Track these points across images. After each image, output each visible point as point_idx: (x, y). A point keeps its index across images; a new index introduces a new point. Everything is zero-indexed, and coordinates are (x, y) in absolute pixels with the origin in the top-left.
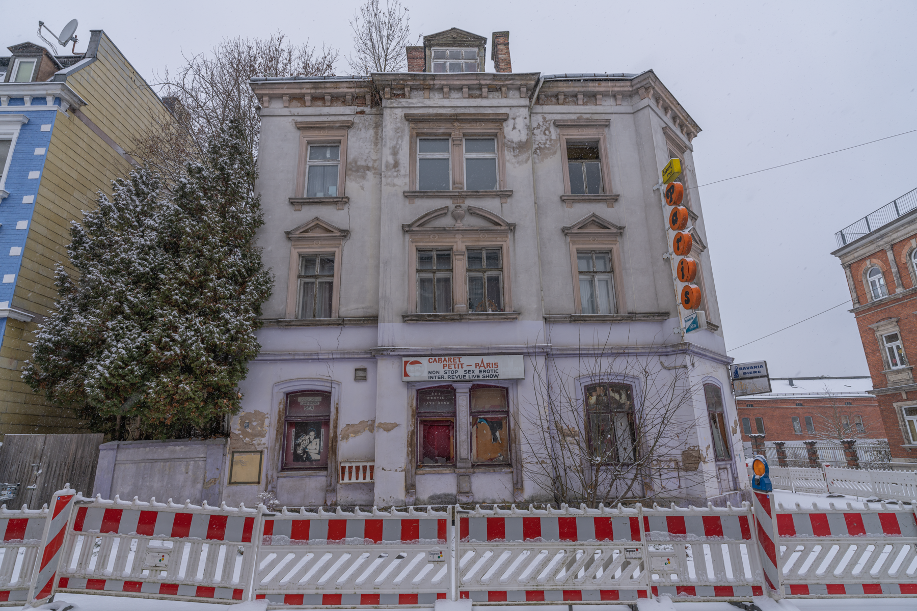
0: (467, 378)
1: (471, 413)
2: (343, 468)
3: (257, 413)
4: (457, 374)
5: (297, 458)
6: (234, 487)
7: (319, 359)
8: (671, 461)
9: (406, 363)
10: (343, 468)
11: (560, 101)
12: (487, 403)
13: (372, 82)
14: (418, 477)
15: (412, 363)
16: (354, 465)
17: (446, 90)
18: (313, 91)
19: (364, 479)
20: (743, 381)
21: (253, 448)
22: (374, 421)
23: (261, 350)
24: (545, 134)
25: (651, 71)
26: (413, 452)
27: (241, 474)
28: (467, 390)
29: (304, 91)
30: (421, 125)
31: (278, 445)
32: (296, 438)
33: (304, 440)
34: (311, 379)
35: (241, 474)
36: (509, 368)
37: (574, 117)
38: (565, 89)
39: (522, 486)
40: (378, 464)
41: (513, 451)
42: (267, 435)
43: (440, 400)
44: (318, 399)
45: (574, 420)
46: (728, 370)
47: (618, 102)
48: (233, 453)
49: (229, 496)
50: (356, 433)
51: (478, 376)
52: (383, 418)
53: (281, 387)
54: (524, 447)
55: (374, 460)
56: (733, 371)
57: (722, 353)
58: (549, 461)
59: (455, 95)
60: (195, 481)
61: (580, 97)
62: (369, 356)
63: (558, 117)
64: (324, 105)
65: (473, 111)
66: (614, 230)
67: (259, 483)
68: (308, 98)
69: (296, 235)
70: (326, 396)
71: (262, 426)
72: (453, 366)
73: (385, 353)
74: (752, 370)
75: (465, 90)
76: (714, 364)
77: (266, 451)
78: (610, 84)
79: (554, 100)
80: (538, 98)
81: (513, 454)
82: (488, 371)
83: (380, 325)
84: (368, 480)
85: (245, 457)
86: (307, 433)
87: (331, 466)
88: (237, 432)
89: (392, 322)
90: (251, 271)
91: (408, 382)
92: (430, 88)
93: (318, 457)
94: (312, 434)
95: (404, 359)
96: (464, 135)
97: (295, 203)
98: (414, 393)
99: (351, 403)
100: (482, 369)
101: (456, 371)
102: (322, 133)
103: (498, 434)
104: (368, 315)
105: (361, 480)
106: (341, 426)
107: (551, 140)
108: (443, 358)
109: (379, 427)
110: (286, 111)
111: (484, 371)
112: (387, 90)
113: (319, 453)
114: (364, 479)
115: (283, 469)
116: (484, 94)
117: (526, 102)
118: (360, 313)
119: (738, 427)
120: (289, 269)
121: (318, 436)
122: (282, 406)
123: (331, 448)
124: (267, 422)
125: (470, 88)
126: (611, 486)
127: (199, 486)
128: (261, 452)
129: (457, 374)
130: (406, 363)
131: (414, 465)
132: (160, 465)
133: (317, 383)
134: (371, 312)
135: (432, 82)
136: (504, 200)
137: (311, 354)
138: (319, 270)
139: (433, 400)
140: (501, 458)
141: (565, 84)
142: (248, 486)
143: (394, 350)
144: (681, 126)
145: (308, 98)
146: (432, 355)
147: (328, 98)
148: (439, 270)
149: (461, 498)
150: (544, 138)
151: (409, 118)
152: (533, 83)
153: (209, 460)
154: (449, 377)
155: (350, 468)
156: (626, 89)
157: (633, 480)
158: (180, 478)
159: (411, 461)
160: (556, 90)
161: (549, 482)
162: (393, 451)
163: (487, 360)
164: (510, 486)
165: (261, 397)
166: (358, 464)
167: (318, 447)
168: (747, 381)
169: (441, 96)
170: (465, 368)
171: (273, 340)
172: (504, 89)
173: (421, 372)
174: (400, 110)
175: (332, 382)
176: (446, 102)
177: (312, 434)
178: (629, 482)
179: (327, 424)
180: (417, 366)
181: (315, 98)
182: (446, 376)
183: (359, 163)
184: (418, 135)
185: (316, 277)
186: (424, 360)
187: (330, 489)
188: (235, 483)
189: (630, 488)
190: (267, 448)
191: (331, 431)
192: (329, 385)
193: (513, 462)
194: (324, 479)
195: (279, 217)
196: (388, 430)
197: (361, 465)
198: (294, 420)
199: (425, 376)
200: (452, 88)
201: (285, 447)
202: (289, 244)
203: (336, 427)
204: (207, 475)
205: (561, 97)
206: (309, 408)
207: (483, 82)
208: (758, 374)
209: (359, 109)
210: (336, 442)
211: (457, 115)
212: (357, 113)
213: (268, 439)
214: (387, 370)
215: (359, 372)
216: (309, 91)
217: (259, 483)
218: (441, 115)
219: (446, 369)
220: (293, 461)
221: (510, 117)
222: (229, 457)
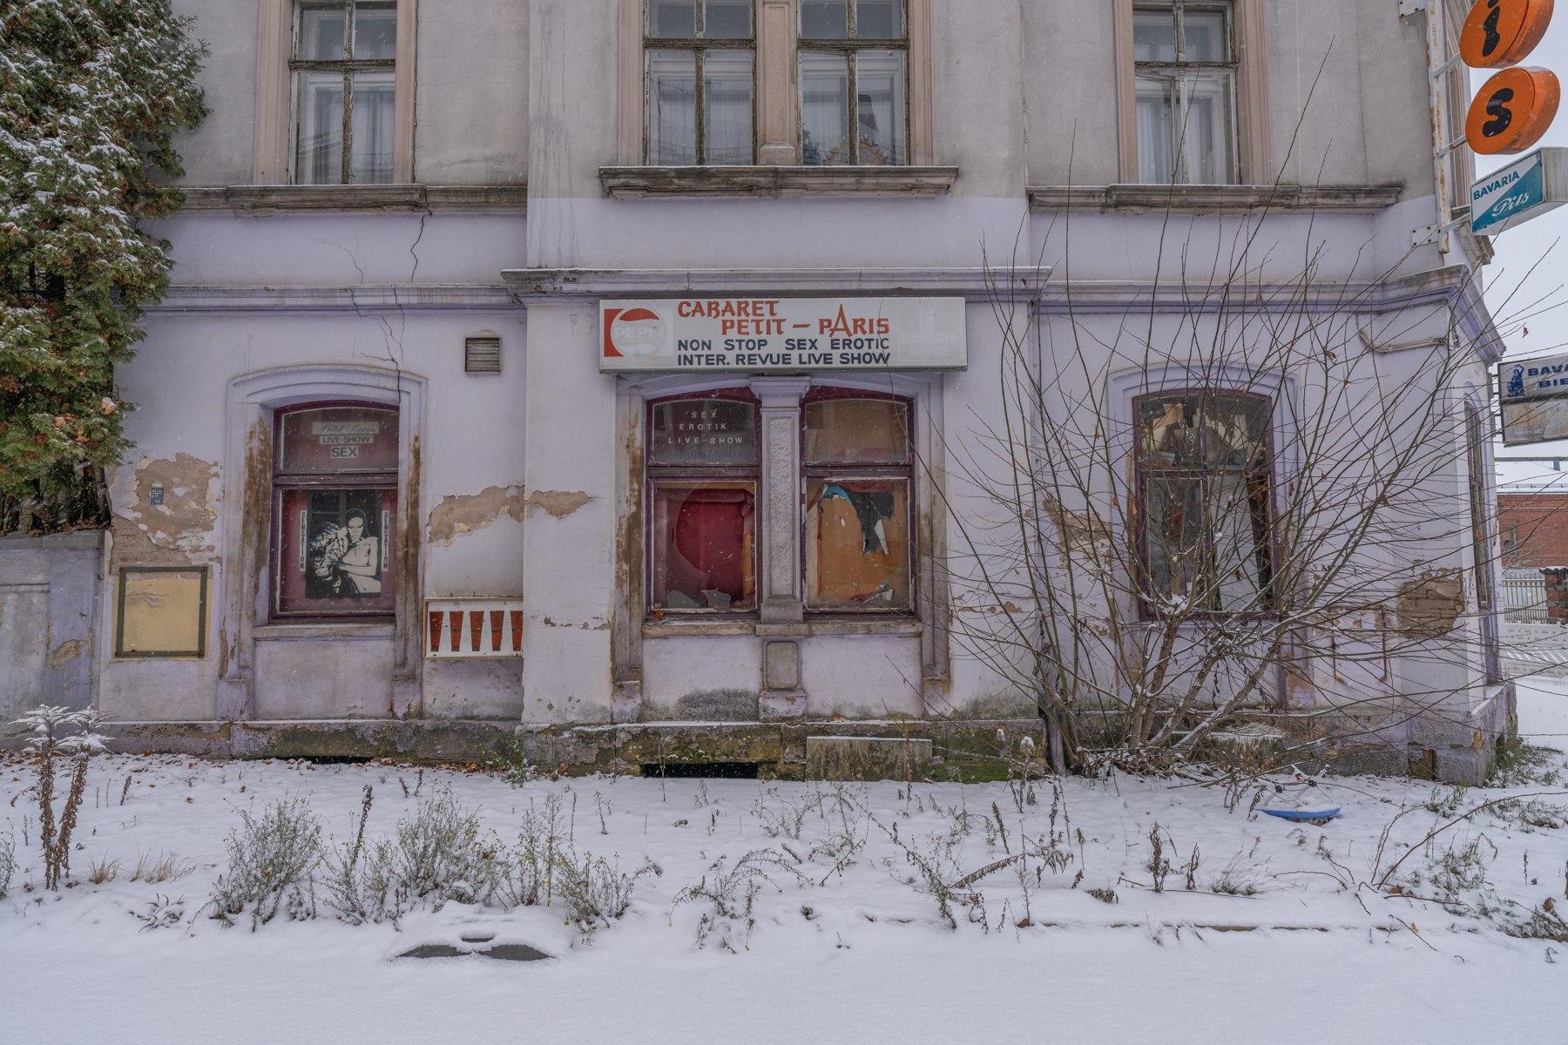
0: (795, 364)
1: (804, 469)
2: (437, 617)
4: (764, 351)
5: (316, 587)
6: (131, 665)
7: (356, 308)
8: (1367, 607)
9: (610, 315)
10: (437, 617)
14: (649, 645)
15: (631, 316)
16: (467, 609)
19: (496, 647)
21: (178, 561)
22: (521, 488)
26: (634, 576)
27: (146, 629)
28: (795, 402)
31: (250, 555)
32: (312, 536)
33: (336, 537)
35: (146, 629)
36: (923, 334)
39: (947, 672)
40: (531, 606)
41: (925, 575)
42: (217, 525)
45: (1104, 494)
48: (123, 572)
50: (475, 521)
51: (827, 358)
52: (544, 478)
53: (250, 388)
54: (959, 565)
55: (520, 598)
58: (1030, 606)
60: (22, 648)
62: (504, 299)
67: (200, 654)
70: (385, 415)
71: (202, 497)
72: (752, 327)
73: (547, 286)
77: (216, 567)
81: (925, 585)
82: (858, 344)
83: (534, 203)
84: (507, 649)
87: (405, 611)
89: (571, 194)
91: (620, 376)
93: (376, 587)
94: (357, 522)
95: (605, 304)
98: (638, 408)
99: (456, 436)
100: (841, 335)
103: (879, 529)
104: (500, 179)
105: (486, 649)
106: (431, 501)
108: (722, 303)
109: (536, 503)
111: (847, 343)
113: (378, 576)
114: (496, 647)
115: (274, 618)
118: (477, 174)
121: (372, 529)
122: (256, 443)
123: (405, 565)
124: (215, 487)
126: (1202, 676)
127: (36, 661)
128: (204, 571)
129: (764, 351)
130: (610, 315)
131: (639, 611)
134: (508, 172)
137: (332, 292)
139: (697, 433)
140: (888, 596)
143: (574, 276)
149: (771, 704)
153: (56, 591)
154: (740, 358)
157: (1266, 661)
159: (628, 602)
161: (1030, 662)
162: (574, 575)
163: (856, 308)
164: (912, 673)
165: (195, 412)
166: (477, 607)
167: (374, 560)
170: (790, 333)
171: (211, 250)
173: (655, 342)
177: (357, 522)
178: (1254, 665)
179: (392, 497)
180: (643, 325)
182: (731, 356)
186: (666, 310)
188: (134, 653)
189: (1253, 682)
190: (219, 559)
191: (402, 515)
192: (392, 384)
193: (925, 605)
194: (387, 645)
196: (559, 512)
197: (487, 609)
199: (668, 356)
203: (415, 504)
204: (54, 631)
206: (341, 453)
210: (417, 544)
213: (221, 532)
214: (555, 342)
217: (200, 654)
219: (733, 334)
220: (303, 597)
222: (111, 583)
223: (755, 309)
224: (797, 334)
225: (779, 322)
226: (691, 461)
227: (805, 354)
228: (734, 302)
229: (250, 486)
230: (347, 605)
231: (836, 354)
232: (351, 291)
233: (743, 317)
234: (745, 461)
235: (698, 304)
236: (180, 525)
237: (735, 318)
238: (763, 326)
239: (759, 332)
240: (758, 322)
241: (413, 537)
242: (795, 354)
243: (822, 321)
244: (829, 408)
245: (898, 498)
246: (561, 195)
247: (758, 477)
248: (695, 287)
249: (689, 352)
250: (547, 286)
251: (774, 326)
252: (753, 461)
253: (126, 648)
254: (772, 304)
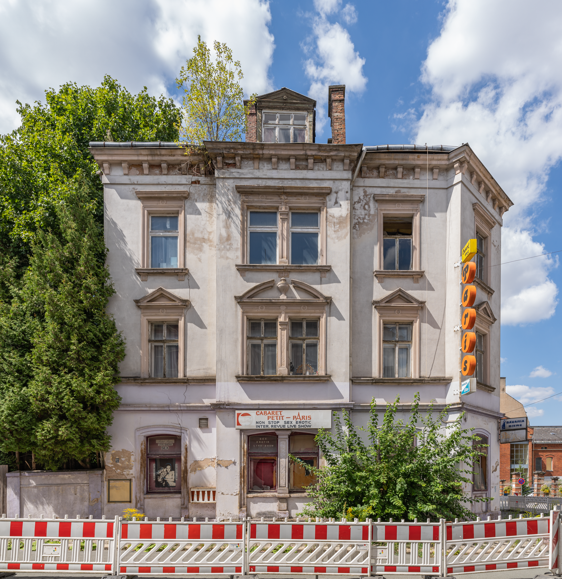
0: (286, 427)
3: (124, 451)
4: (278, 424)
5: (158, 484)
7: (170, 410)
9: (238, 415)
10: (193, 492)
11: (382, 174)
12: (302, 447)
13: (205, 149)
15: (243, 415)
17: (274, 160)
18: (150, 158)
20: (507, 432)
21: (123, 477)
23: (122, 402)
24: (365, 209)
25: (467, 145)
27: (116, 495)
28: (287, 437)
29: (141, 158)
30: (251, 198)
31: (142, 476)
32: (156, 471)
33: (163, 472)
34: (165, 426)
37: (392, 191)
38: (387, 162)
42: (134, 468)
43: (267, 444)
44: (172, 441)
46: (499, 423)
47: (435, 177)
49: (109, 511)
51: (295, 426)
53: (141, 432)
56: (502, 424)
57: (495, 409)
59: (283, 165)
60: (82, 500)
61: (400, 170)
63: (378, 191)
64: (161, 174)
65: (299, 184)
66: (415, 305)
67: (130, 502)
68: (145, 165)
69: (144, 303)
70: (177, 439)
71: (129, 461)
72: (275, 418)
74: (516, 424)
75: (293, 160)
76: (486, 419)
77: (134, 479)
78: (428, 156)
79: (375, 173)
80: (361, 170)
82: (303, 422)
83: (218, 383)
84: (211, 501)
85: (118, 483)
86: (165, 467)
87: (183, 490)
88: (110, 465)
89: (228, 381)
90: (106, 336)
92: (260, 158)
93: (174, 484)
94: (169, 467)
95: (237, 412)
96: (290, 209)
97: (142, 273)
100: (299, 420)
101: (278, 422)
102: (161, 203)
107: (369, 215)
108: (268, 411)
110: (125, 180)
111: (300, 422)
112: (219, 159)
113: (175, 481)
114: (209, 500)
115: (148, 493)
116: (310, 166)
117: (347, 175)
119: (498, 468)
120: (141, 334)
121: (173, 469)
122: (143, 447)
124: (132, 458)
125: (297, 158)
127: (86, 503)
128: (130, 480)
129: (278, 424)
130: (238, 415)
132: (55, 488)
133: (170, 429)
135: (261, 152)
136: (323, 275)
137: (163, 407)
138: (165, 335)
139: (261, 444)
141: (386, 156)
142: (123, 504)
143: (229, 404)
144: (494, 200)
145: (145, 165)
146: (258, 408)
147: (164, 165)
148: (265, 338)
150: (363, 212)
151: (242, 191)
152: (356, 154)
153: (91, 485)
154: (272, 426)
155: (198, 492)
156: (444, 162)
158: (71, 498)
160: (377, 162)
163: (303, 413)
165: (127, 439)
167: (173, 477)
168: (511, 432)
169: (270, 166)
170: (285, 419)
172: (328, 160)
173: (251, 421)
174: (232, 181)
175: (181, 428)
176: (274, 174)
177: (169, 467)
179: (179, 460)
181: (153, 166)
183: (196, 235)
184: (248, 207)
185: (163, 341)
187: (184, 507)
190: (134, 477)
191: (183, 466)
192: (179, 431)
195: (128, 288)
198: (154, 457)
199: (254, 426)
200: (280, 159)
201: (148, 477)
202: (139, 312)
203: (186, 463)
204: (91, 496)
205: (382, 170)
207: (309, 153)
208: (519, 427)
209: (195, 178)
210: (187, 473)
211: (283, 188)
212: (192, 183)
213: (134, 470)
215: (203, 421)
216: (145, 158)
217: (130, 502)
218: (269, 187)
220: (156, 487)
221: (333, 190)
222: (106, 483)
225: (282, 417)
226: (260, 452)
228: (271, 411)
229: (142, 458)
230: (166, 490)
231: (297, 425)
232: (169, 406)
234: (274, 452)
236: (123, 468)
238: (278, 418)
241: (186, 471)
242: (286, 425)
245: (315, 462)
246: (225, 381)
247: (277, 456)
248: (261, 407)
249: (259, 425)
250: (222, 407)
253: (111, 500)
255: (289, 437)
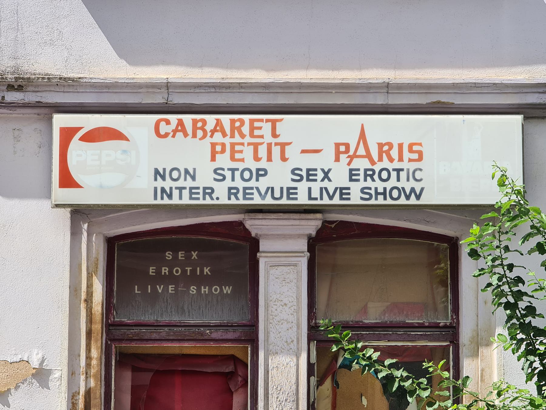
0: (302, 199)
1: (313, 331)
4: (263, 183)
9: (68, 134)
15: (92, 137)
28: (303, 245)
43: (201, 280)
51: (343, 192)
72: (248, 152)
82: (384, 175)
95: (61, 120)
100: (362, 164)
101: (261, 173)
108: (211, 119)
111: (369, 174)
129: (263, 183)
130: (68, 134)
139: (170, 279)
143: (19, 85)
146: (164, 105)
154: (232, 192)
163: (381, 128)
199: (140, 190)
219: (224, 161)
223: (252, 129)
224: (305, 162)
225: (283, 146)
226: (165, 319)
227: (316, 187)
228: (225, 119)
231: (355, 189)
233: (237, 139)
234: (236, 319)
235: (180, 123)
237: (227, 141)
238: (263, 152)
239: (257, 158)
240: (256, 146)
242: (303, 187)
243: (337, 145)
244: (345, 254)
247: (253, 341)
248: (178, 99)
249: (168, 184)
251: (276, 151)
252: (246, 319)
254: (274, 123)
255: (313, 243)
